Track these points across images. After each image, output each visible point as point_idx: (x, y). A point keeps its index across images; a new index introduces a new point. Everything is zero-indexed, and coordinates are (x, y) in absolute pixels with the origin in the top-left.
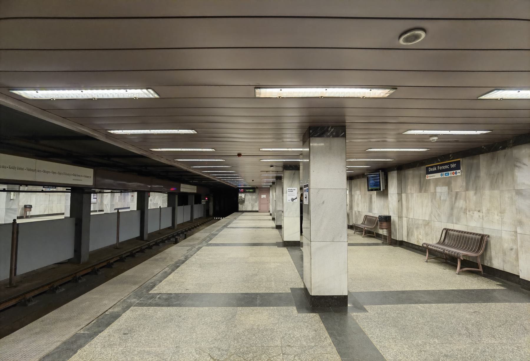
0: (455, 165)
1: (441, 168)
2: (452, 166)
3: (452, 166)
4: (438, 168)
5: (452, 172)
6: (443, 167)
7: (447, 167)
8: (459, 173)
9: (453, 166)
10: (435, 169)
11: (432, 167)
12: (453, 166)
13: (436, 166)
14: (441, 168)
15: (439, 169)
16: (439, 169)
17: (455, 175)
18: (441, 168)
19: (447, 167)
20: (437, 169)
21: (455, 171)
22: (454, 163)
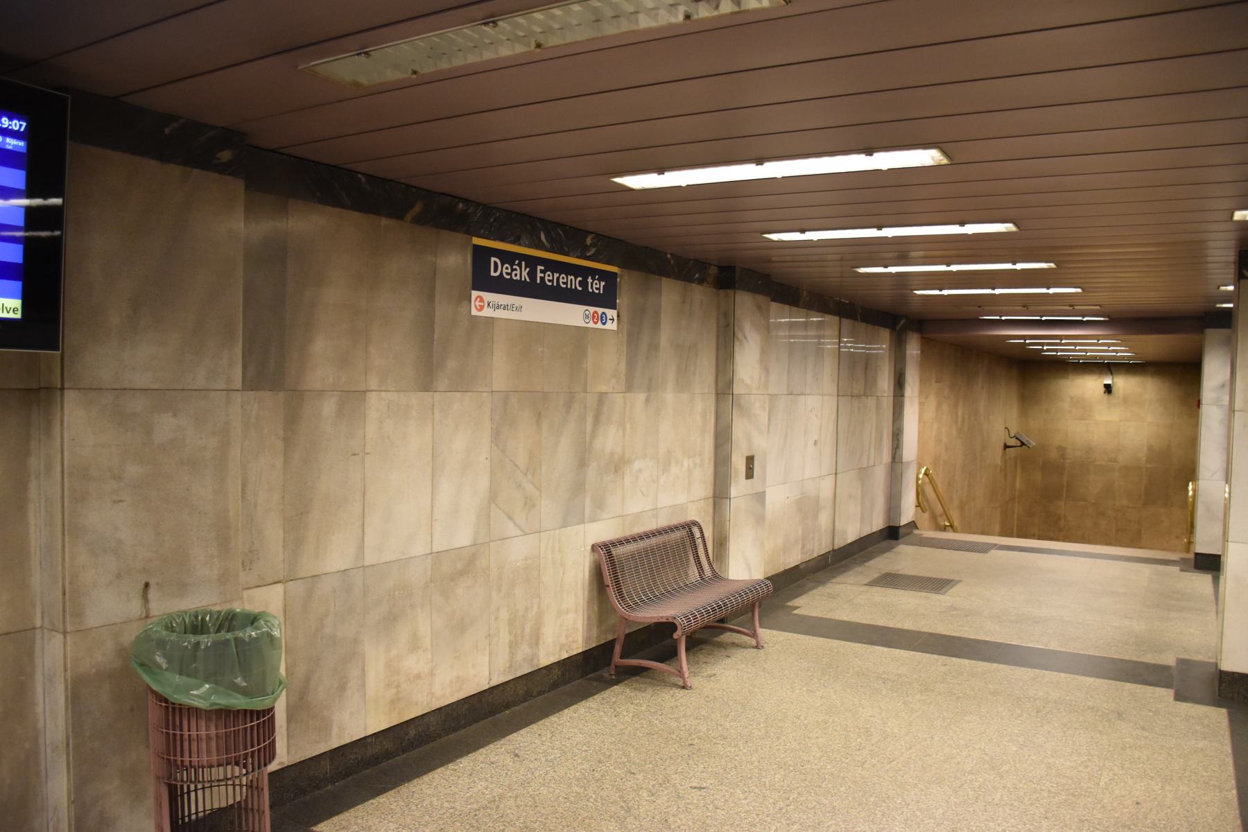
0: (603, 284)
1: (551, 281)
2: (592, 288)
3: (592, 288)
4: (539, 275)
5: (592, 309)
6: (561, 280)
7: (573, 282)
8: (613, 320)
9: (596, 286)
10: (522, 274)
11: (508, 258)
12: (594, 286)
13: (532, 262)
14: (550, 278)
15: (542, 279)
16: (542, 279)
17: (599, 325)
18: (550, 278)
19: (573, 282)
20: (532, 274)
21: (600, 310)
22: (603, 275)
